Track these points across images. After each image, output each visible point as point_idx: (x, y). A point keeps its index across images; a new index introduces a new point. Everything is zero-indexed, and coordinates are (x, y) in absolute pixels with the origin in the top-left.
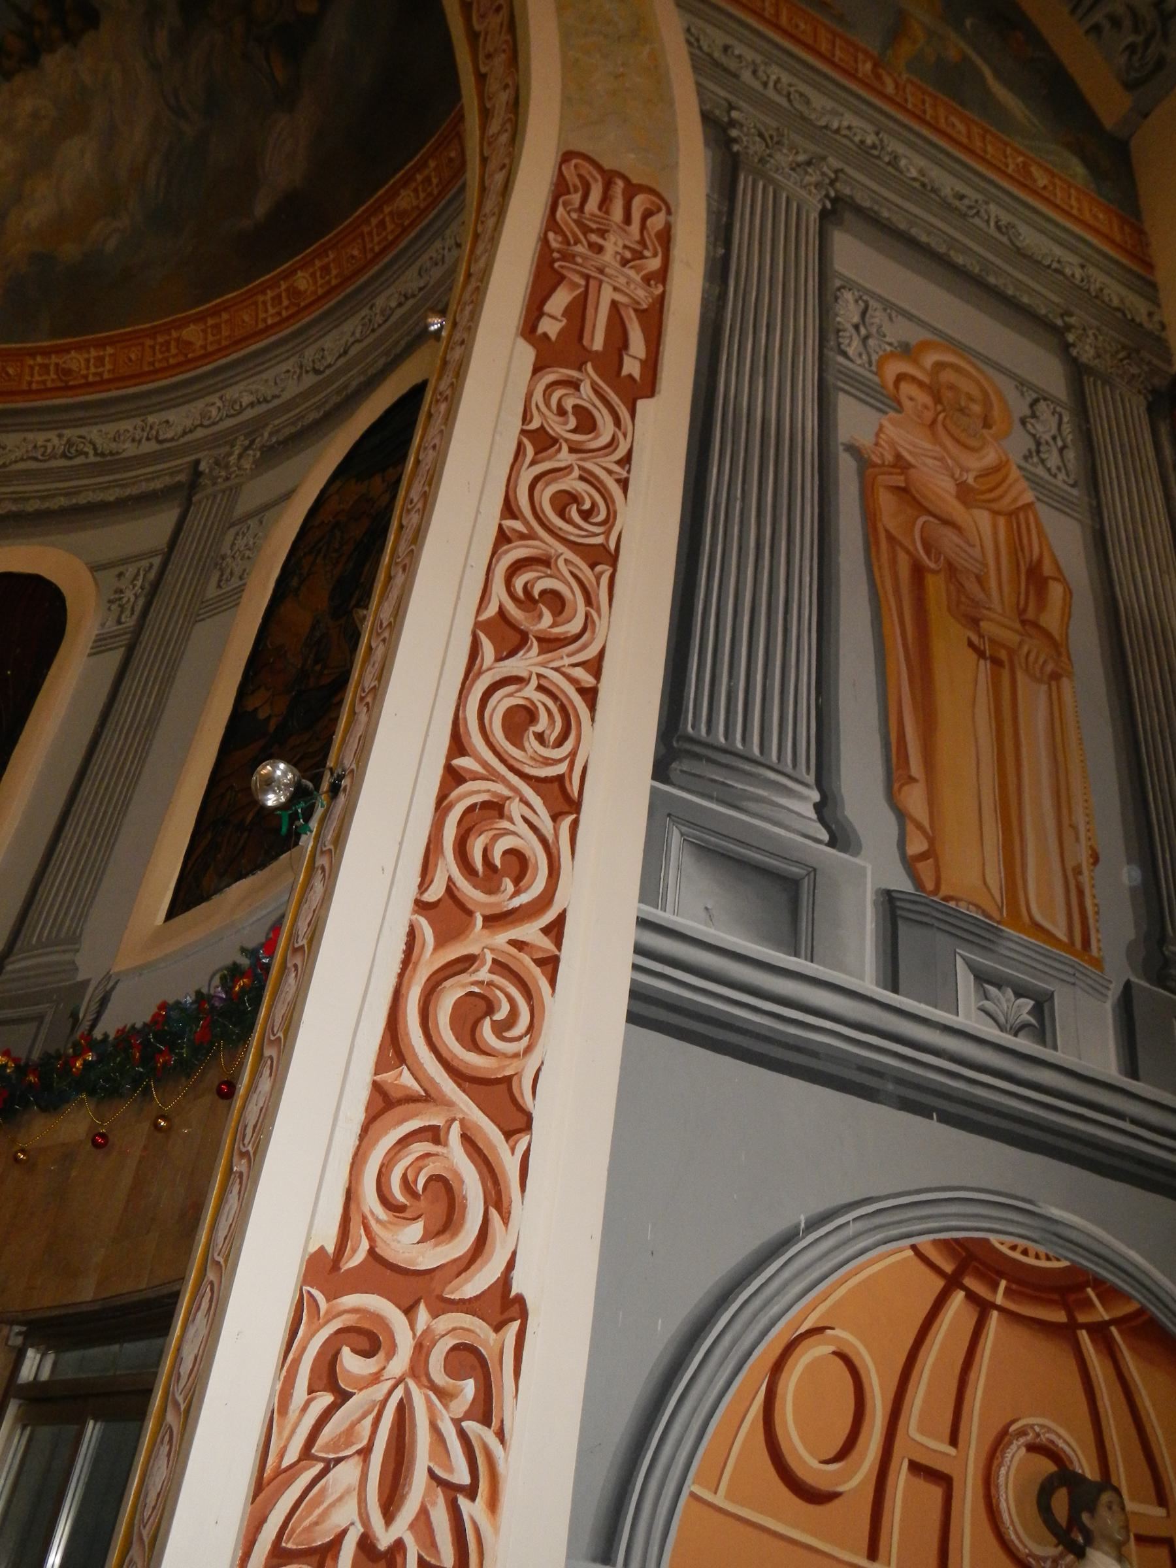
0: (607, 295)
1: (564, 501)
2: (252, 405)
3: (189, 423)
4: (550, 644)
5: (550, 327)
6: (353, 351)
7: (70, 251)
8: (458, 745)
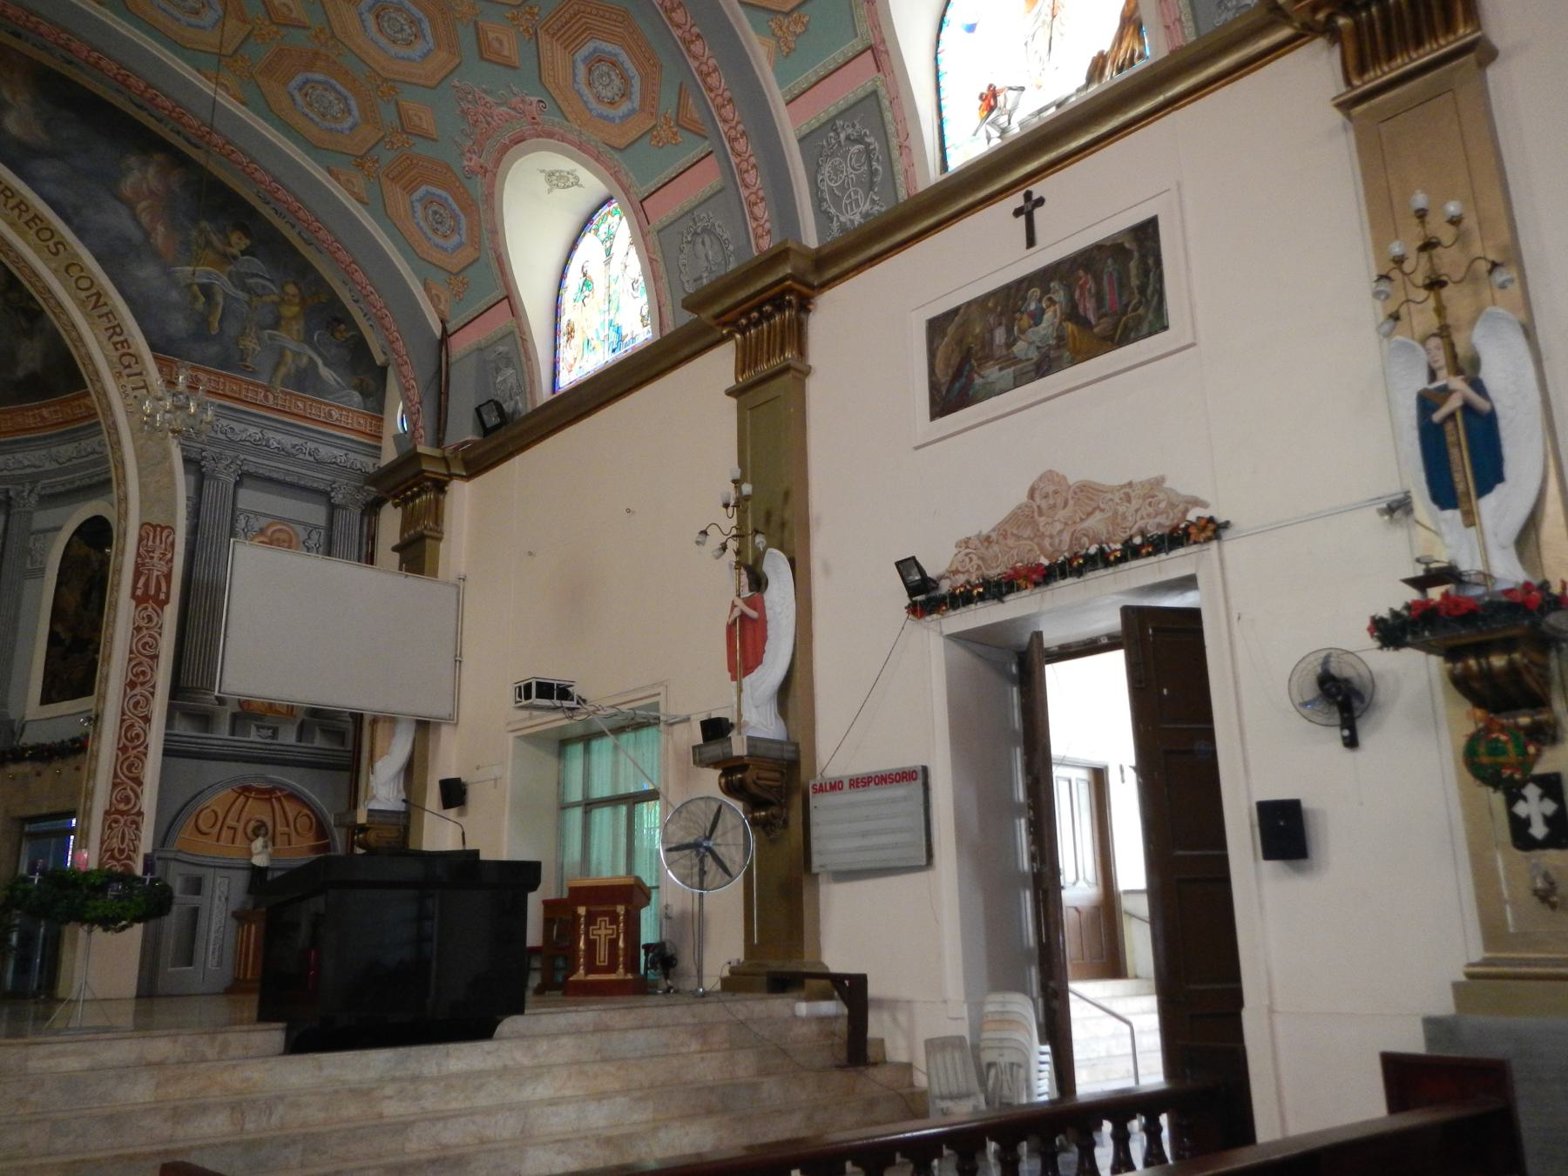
0: (156, 573)
2: (28, 466)
4: (144, 683)
5: (139, 592)
6: (75, 461)
8: (123, 713)
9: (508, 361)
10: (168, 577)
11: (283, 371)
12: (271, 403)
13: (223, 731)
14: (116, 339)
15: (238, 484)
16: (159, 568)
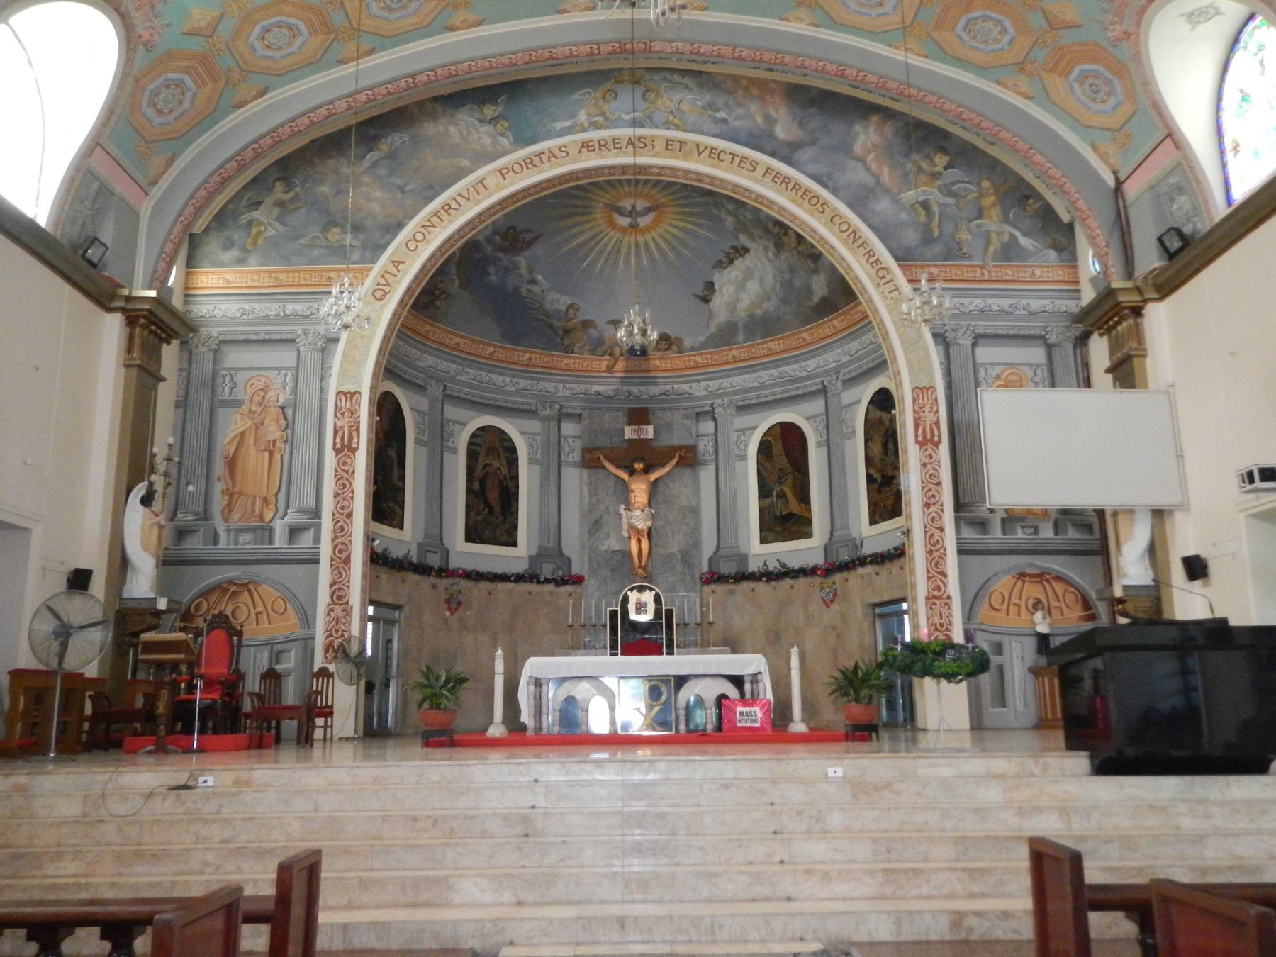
0: (928, 423)
1: (931, 475)
3: (816, 366)
4: (934, 504)
5: (920, 438)
6: (860, 352)
7: (759, 312)
8: (925, 527)
9: (1180, 190)
10: (937, 423)
11: (991, 249)
12: (987, 277)
13: (997, 533)
14: (872, 260)
15: (974, 345)
16: (930, 419)
